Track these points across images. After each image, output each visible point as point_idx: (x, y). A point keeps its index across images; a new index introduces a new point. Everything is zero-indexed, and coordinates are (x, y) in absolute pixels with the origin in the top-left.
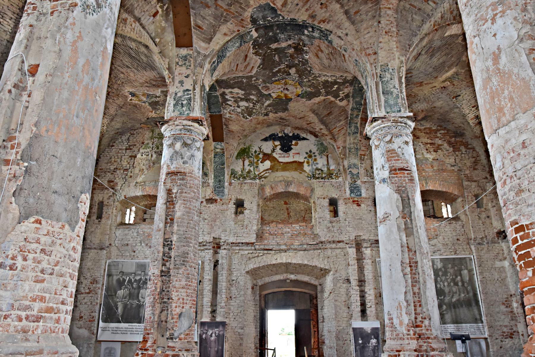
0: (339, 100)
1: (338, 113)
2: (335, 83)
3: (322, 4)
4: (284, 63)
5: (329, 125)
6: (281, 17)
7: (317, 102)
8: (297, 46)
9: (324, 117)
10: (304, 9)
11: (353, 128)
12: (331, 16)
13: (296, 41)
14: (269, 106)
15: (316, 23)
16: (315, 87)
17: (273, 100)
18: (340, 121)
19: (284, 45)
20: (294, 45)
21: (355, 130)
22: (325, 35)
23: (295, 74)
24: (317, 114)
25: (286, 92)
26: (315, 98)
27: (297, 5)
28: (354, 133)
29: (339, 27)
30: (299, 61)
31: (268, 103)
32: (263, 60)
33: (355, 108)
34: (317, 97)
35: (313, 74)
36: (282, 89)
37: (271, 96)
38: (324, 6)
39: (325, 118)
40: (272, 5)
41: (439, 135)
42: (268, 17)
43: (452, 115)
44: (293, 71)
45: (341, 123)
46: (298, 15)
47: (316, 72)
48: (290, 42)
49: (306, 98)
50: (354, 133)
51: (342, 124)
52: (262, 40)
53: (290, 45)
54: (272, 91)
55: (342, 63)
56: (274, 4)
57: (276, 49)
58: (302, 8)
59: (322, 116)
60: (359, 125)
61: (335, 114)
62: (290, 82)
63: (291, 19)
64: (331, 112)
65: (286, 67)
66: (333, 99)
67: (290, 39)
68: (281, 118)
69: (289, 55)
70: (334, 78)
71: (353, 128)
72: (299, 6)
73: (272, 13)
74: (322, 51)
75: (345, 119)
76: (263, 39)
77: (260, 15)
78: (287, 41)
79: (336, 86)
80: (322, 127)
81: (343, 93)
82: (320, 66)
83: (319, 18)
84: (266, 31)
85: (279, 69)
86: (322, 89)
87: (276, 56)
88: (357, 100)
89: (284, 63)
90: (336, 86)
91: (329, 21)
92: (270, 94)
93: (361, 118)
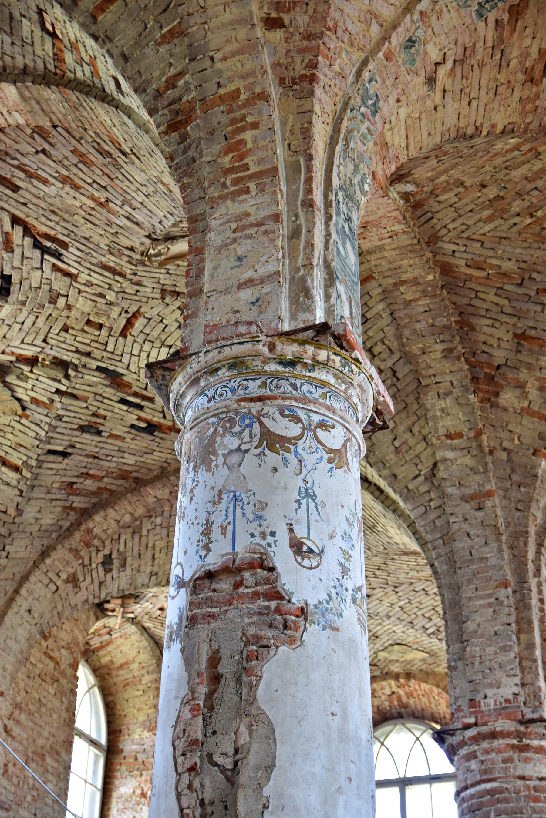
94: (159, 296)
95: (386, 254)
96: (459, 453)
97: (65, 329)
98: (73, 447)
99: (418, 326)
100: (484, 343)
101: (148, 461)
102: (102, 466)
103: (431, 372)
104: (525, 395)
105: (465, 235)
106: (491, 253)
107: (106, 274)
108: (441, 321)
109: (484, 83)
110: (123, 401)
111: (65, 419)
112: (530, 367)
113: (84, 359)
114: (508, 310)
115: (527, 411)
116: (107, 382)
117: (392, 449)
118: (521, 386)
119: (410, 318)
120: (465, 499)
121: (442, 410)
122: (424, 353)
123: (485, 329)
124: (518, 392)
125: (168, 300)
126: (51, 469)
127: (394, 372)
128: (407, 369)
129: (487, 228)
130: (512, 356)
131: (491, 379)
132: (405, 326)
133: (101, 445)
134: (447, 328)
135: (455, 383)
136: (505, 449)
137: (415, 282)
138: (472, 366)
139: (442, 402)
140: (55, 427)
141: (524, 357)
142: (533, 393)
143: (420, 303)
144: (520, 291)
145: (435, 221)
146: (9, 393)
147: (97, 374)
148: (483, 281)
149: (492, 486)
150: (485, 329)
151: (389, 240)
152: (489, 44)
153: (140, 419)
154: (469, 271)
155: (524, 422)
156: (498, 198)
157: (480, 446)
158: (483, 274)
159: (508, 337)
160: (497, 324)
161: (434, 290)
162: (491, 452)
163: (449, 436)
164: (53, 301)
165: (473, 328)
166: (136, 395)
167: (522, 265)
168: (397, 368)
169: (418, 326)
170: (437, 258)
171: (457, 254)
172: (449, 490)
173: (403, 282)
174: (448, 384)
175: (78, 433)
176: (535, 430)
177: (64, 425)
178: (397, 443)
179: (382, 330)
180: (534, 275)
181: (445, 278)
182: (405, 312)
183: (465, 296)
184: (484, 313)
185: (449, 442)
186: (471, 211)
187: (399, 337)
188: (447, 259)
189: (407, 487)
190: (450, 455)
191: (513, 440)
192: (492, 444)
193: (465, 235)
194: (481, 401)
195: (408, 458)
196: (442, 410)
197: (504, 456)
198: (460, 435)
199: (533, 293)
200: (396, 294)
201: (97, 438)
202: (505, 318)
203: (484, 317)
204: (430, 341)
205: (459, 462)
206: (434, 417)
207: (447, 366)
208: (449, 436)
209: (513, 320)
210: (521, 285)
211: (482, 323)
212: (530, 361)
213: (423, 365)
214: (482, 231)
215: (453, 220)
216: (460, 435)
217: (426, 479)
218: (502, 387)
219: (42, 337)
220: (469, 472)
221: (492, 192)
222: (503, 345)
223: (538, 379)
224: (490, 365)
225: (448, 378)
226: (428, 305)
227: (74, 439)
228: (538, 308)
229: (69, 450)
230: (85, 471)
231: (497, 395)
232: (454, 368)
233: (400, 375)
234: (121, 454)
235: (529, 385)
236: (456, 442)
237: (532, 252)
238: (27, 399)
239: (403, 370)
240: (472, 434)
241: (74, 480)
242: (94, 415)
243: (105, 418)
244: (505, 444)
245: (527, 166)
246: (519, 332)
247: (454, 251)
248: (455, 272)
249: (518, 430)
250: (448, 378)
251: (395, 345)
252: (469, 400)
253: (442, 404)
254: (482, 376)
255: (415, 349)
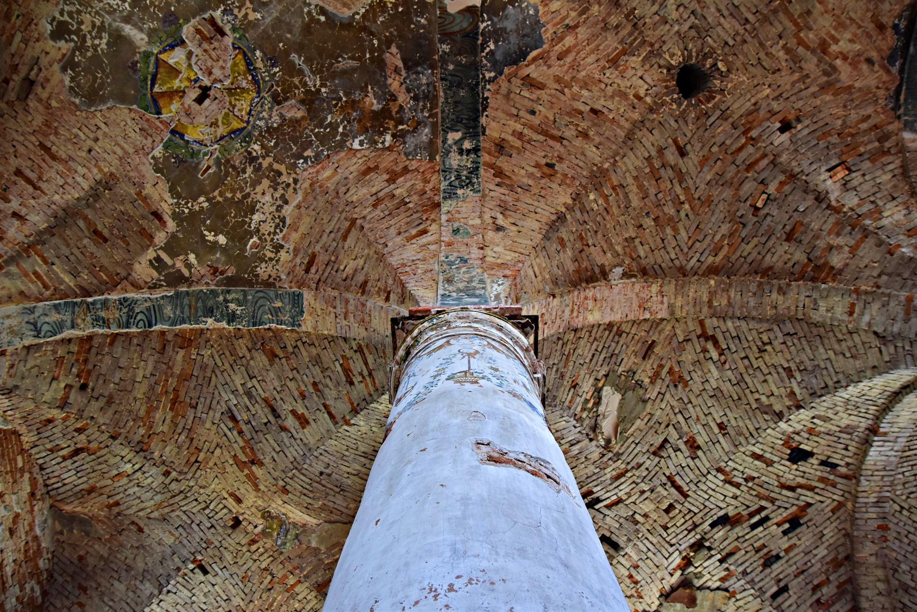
0: (158, 259)
1: (105, 261)
2: (240, 235)
3: (550, 166)
4: (322, 85)
5: (55, 240)
6: (493, 74)
7: (148, 190)
8: (391, 118)
9: (85, 218)
10: (519, 127)
11: (54, 317)
12: (527, 189)
13: (408, 115)
14: (118, 39)
15: (485, 157)
16: (218, 181)
17: (147, 55)
18: (75, 274)
19: (394, 83)
20: (394, 110)
21: (45, 328)
22: (468, 179)
23: (282, 116)
24: (94, 194)
25: (194, 94)
26: (164, 186)
27: (533, 113)
28: (35, 324)
29: (504, 209)
30: (334, 127)
31: (139, 37)
32: (347, 25)
33: (132, 310)
34: (172, 190)
35: (294, 166)
36: (206, 82)
37: (172, 47)
38: (546, 170)
39: (81, 223)
40: (534, 53)
41: (28, 587)
42: (496, 43)
43: (120, 587)
44: (294, 111)
45: (67, 279)
46: (499, 114)
47: (305, 172)
48: (403, 98)
49: (166, 159)
50: (35, 324)
51: (62, 282)
52: (419, 25)
53: (394, 98)
54: (197, 51)
55: (393, 231)
56: (535, 59)
57: (380, 63)
58: (524, 125)
59: (89, 213)
60: (67, 333)
61: (99, 253)
62: (243, 105)
63: (487, 98)
64: (106, 240)
65: (308, 92)
66: (160, 238)
67: (416, 98)
68: (29, 84)
69: (357, 96)
70: (267, 228)
71: (54, 317)
72: (529, 117)
73: (507, 54)
74: (391, 180)
75: (81, 288)
76: (423, 27)
77: (509, 25)
78: (408, 91)
79: (222, 239)
80: (38, 220)
81: (189, 266)
82: (337, 178)
83: (503, 163)
84: (458, 38)
85: (301, 72)
86: (208, 200)
87: (354, 63)
88: (168, 311)
89: (322, 85)
90: (222, 239)
91: (511, 188)
92: (183, 42)
93: (90, 338)
94: (657, 459)
95: (679, 304)
96: (867, 311)
97: (666, 528)
98: (780, 580)
99: (752, 304)
100: (786, 263)
101: (831, 541)
102: (815, 573)
103: (793, 308)
104: (839, 248)
105: (686, 250)
106: (709, 238)
107: (623, 480)
108: (753, 287)
109: (530, 201)
110: (754, 527)
111: (749, 570)
112: (816, 237)
113: (699, 530)
114: (763, 240)
115: (853, 250)
116: (728, 527)
117: (851, 360)
118: (830, 248)
119: (743, 307)
120: (907, 320)
121: (828, 311)
122: (776, 307)
123: (774, 259)
124: (834, 252)
125: (665, 454)
126: (790, 606)
127: (788, 334)
128: (789, 325)
129: (683, 233)
130: (802, 248)
131: (818, 268)
132: (749, 313)
133: (791, 562)
134: (760, 284)
135: (808, 294)
136: (879, 276)
137: (712, 294)
138: (802, 277)
139: (821, 309)
140: (752, 580)
141: (806, 239)
142: (840, 241)
143: (732, 295)
144: (749, 227)
145: (663, 265)
146: (708, 591)
147: (716, 530)
148: (732, 250)
149: (903, 295)
150: (774, 259)
151: (665, 298)
152: (507, 192)
153: (778, 525)
154: (721, 255)
155: (861, 254)
156: (656, 219)
157: (866, 293)
158: (726, 248)
159: (786, 246)
160: (773, 250)
161: (725, 283)
162: (878, 287)
163: (851, 313)
164: (636, 523)
165: (771, 268)
166: (751, 515)
167: (728, 219)
168: (786, 331)
169: (752, 304)
170: (700, 272)
171: (702, 259)
172: (896, 329)
173: (710, 302)
174: (807, 300)
175: (768, 571)
176: (871, 248)
177: (753, 574)
178: (848, 355)
179: (750, 330)
180: (739, 214)
181: (721, 273)
182: (737, 307)
183: (741, 266)
184: (760, 257)
185: (855, 315)
186: (663, 240)
187: (761, 321)
188: (704, 267)
189: (887, 362)
190: (866, 318)
191: (874, 267)
192: (871, 284)
193: (686, 250)
194: (834, 281)
195: (862, 351)
196: (828, 311)
197: (884, 278)
198: (853, 305)
199: (755, 219)
200: (718, 309)
201: (783, 561)
202: (770, 244)
203: (764, 257)
204: (767, 300)
205: (874, 313)
206: (832, 319)
207: (792, 295)
208: (851, 313)
209: (773, 239)
210: (744, 225)
211: (768, 260)
212: (811, 236)
213: (786, 311)
214: (686, 239)
215: (668, 253)
216: (853, 305)
217: (884, 344)
218: (826, 263)
219: (667, 546)
220: (885, 309)
221: (648, 222)
222: (791, 251)
223: (829, 234)
224: (806, 265)
225: (802, 298)
226: (736, 291)
227: (773, 575)
228: (769, 219)
229: (782, 584)
230: (810, 586)
231: (832, 268)
232: (796, 291)
233: (792, 331)
234: (811, 555)
235: (831, 242)
236: (857, 310)
237: (717, 211)
238: (718, 584)
239: (789, 328)
240: (854, 296)
241: (815, 598)
242: (757, 551)
243: (764, 546)
244: (875, 274)
245: (631, 196)
246: (784, 237)
247: (698, 261)
248: (718, 266)
249: (866, 261)
250: (802, 298)
251: (766, 326)
252: (824, 289)
253: (822, 309)
254: (812, 273)
255: (770, 312)
